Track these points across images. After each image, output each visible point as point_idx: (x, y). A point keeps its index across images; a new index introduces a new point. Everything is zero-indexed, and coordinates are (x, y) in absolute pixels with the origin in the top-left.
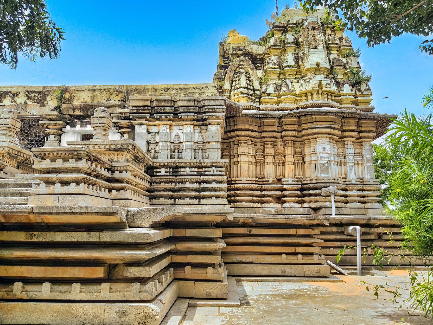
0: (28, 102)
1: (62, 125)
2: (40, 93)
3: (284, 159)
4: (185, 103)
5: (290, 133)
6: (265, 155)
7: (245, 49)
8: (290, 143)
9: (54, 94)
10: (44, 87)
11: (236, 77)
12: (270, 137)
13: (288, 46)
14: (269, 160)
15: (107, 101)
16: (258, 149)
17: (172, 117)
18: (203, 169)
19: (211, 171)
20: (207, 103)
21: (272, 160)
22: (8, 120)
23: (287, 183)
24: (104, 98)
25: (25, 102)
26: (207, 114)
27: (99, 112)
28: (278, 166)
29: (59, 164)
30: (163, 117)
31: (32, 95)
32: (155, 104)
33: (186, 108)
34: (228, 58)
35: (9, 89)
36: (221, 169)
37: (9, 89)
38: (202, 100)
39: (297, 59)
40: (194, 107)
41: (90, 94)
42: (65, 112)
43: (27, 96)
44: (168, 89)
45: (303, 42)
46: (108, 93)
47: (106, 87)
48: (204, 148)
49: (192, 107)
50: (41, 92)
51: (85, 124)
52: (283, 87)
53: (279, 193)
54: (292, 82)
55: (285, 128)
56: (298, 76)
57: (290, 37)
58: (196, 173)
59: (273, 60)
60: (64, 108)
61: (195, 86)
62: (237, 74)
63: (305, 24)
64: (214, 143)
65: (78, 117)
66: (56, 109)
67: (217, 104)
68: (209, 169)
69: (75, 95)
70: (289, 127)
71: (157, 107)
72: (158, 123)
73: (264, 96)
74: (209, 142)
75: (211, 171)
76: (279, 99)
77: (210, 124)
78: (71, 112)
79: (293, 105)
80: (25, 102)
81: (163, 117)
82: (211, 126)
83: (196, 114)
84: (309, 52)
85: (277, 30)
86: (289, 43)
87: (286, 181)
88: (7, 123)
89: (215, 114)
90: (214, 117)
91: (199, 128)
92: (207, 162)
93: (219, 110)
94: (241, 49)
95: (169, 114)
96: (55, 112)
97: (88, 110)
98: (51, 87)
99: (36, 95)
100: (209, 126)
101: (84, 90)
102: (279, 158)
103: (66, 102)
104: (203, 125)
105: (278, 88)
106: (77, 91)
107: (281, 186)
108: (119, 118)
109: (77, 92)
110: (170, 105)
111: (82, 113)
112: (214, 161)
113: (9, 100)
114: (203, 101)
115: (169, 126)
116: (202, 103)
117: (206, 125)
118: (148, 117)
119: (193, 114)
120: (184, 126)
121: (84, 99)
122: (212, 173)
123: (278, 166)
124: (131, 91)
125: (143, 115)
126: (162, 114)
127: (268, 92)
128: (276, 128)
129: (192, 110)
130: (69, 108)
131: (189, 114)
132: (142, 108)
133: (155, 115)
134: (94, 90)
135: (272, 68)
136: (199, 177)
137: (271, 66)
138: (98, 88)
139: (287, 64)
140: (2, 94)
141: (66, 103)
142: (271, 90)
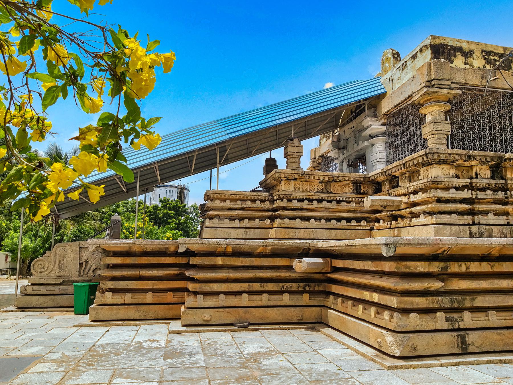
0: (488, 67)
2: (501, 56)
25: (485, 67)
31: (492, 58)
35: (458, 45)
37: (457, 43)
43: (485, 59)
50: (502, 54)
80: (485, 67)
99: (496, 58)
140: (450, 50)
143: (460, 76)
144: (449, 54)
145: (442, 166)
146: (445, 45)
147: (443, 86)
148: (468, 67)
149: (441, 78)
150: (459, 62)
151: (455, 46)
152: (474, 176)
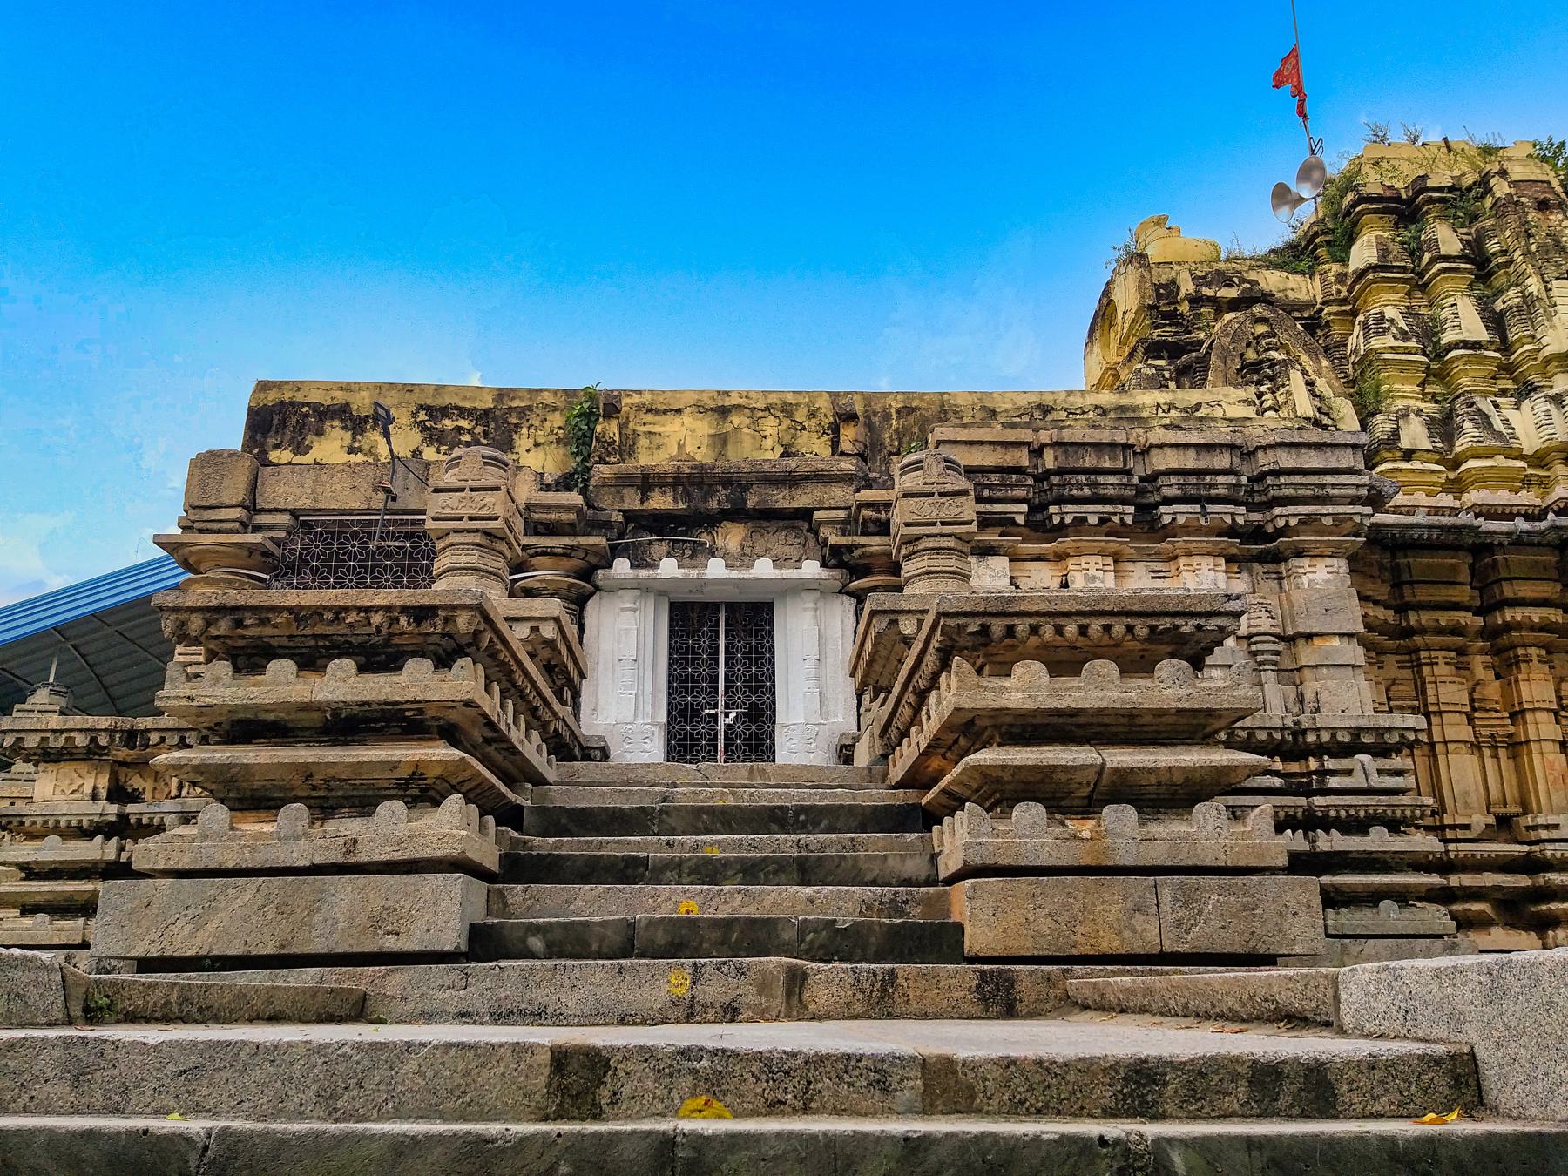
0: (429, 454)
1: (596, 554)
2: (483, 416)
3: (1512, 729)
4: (1190, 461)
5: (1536, 615)
6: (1431, 708)
7: (1248, 281)
8: (1535, 658)
9: (547, 424)
10: (501, 394)
11: (1259, 383)
12: (1440, 631)
13: (1445, 270)
14: (1451, 734)
15: (782, 456)
16: (1394, 681)
17: (1129, 520)
18: (1313, 764)
19: (1349, 772)
20: (1286, 460)
21: (1466, 733)
22: (490, 498)
23: (1554, 834)
24: (769, 443)
25: (417, 453)
26: (1292, 509)
27: (935, 471)
28: (1489, 762)
29: (1100, 688)
30: (1093, 520)
31: (448, 424)
32: (1049, 460)
33: (1193, 480)
34: (1173, 316)
35: (340, 397)
36: (1396, 762)
37: (339, 394)
38: (1264, 448)
39: (1496, 322)
40: (1232, 479)
41: (704, 427)
42: (606, 501)
43: (424, 429)
44: (1046, 410)
45: (1504, 252)
46: (787, 422)
47: (773, 399)
48: (1286, 663)
49: (1221, 479)
50: (487, 411)
51: (688, 552)
52: (1467, 425)
53: (1523, 881)
54: (1496, 406)
55: (1508, 591)
56: (1508, 384)
57: (1448, 239)
58: (1277, 782)
59: (1392, 321)
60: (605, 483)
61: (1162, 401)
62: (1257, 371)
63: (1501, 189)
64: (1336, 642)
65: (660, 524)
66: (565, 483)
67: (1333, 464)
68: (1344, 763)
69: (640, 429)
70: (1526, 590)
71: (1060, 472)
72: (1067, 543)
73: (1383, 461)
74: (1309, 637)
75: (1349, 772)
76: (1452, 476)
77: (1299, 554)
78: (632, 501)
79: (1527, 498)
80: (417, 453)
81: (1093, 520)
82: (1306, 562)
83: (1242, 510)
84: (1548, 290)
85: (1375, 211)
86: (1447, 258)
87: (1547, 827)
88: (484, 512)
89: (1331, 509)
90: (1328, 521)
91: (1245, 575)
92: (1334, 731)
93: (1344, 492)
94: (1230, 279)
95: (1120, 508)
96: (575, 497)
97: (710, 492)
98: (530, 391)
100: (1294, 562)
101: (678, 411)
102: (1497, 721)
103: (609, 454)
104: (1262, 558)
105: (1444, 427)
106: (649, 411)
107: (1526, 848)
108: (844, 527)
109: (650, 418)
110: (1119, 464)
111: (681, 506)
112: (1363, 723)
113: (338, 443)
114: (1270, 453)
115: (1110, 560)
116: (1265, 461)
117: (1277, 558)
118: (1021, 520)
119: (1231, 508)
120: (1182, 561)
121: (681, 446)
122: (1357, 781)
123: (1489, 762)
124: (887, 417)
125: (999, 508)
126: (1085, 508)
127: (1405, 443)
128: (1464, 594)
129: (1222, 491)
130: (623, 481)
131: (1211, 508)
132: (995, 479)
133: (1053, 509)
134: (723, 412)
135: (1393, 349)
136: (1302, 801)
137: (1389, 341)
138: (742, 401)
139: (1460, 337)
140: (306, 415)
141: (612, 459)
142: (1415, 434)
143: (298, 491)
144: (301, 429)
145: (67, 768)
146: (292, 404)
147: (216, 526)
148: (360, 458)
149: (212, 501)
150: (331, 447)
151: (329, 402)
152: (174, 792)
